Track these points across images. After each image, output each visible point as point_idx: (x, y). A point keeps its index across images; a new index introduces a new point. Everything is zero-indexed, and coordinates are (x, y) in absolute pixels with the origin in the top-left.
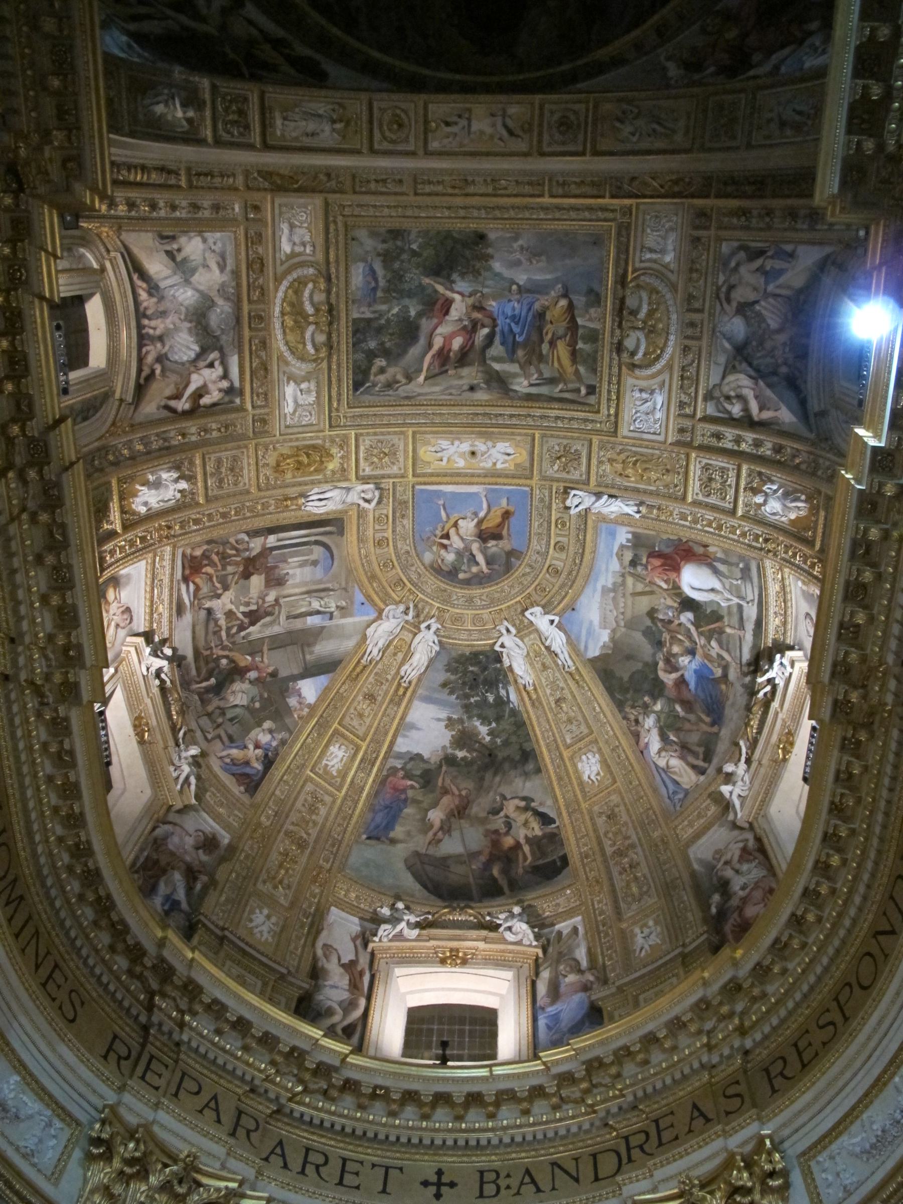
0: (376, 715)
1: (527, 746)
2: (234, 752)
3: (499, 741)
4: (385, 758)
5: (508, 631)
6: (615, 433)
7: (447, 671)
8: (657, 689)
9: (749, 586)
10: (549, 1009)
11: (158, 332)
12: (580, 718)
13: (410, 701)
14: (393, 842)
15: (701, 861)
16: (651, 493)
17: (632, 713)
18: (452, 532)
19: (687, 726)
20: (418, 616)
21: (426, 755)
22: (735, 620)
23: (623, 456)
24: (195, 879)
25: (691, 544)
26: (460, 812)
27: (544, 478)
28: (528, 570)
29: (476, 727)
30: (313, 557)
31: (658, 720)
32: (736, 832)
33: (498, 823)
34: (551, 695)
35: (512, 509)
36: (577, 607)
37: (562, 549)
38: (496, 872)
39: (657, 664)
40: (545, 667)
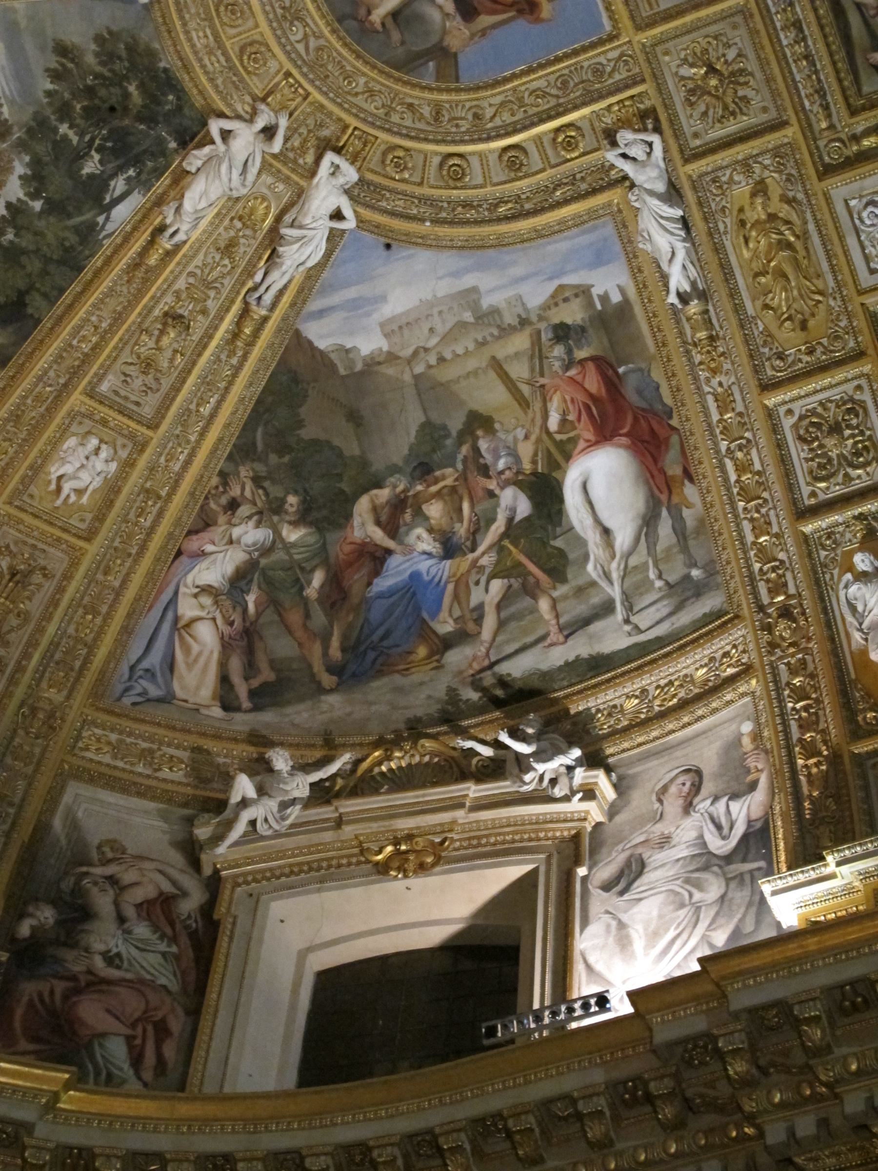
1: (35, 302)
3: (10, 236)
5: (269, 132)
6: (827, 171)
7: (99, 39)
9: (663, 608)
12: (166, 383)
15: (73, 825)
16: (739, 309)
19: (295, 617)
22: (574, 610)
23: (785, 211)
25: (675, 439)
27: (650, 53)
28: (426, 111)
29: (9, 170)
31: (267, 550)
32: (177, 858)
34: (177, 294)
36: (400, 252)
39: (379, 485)
40: (229, 249)
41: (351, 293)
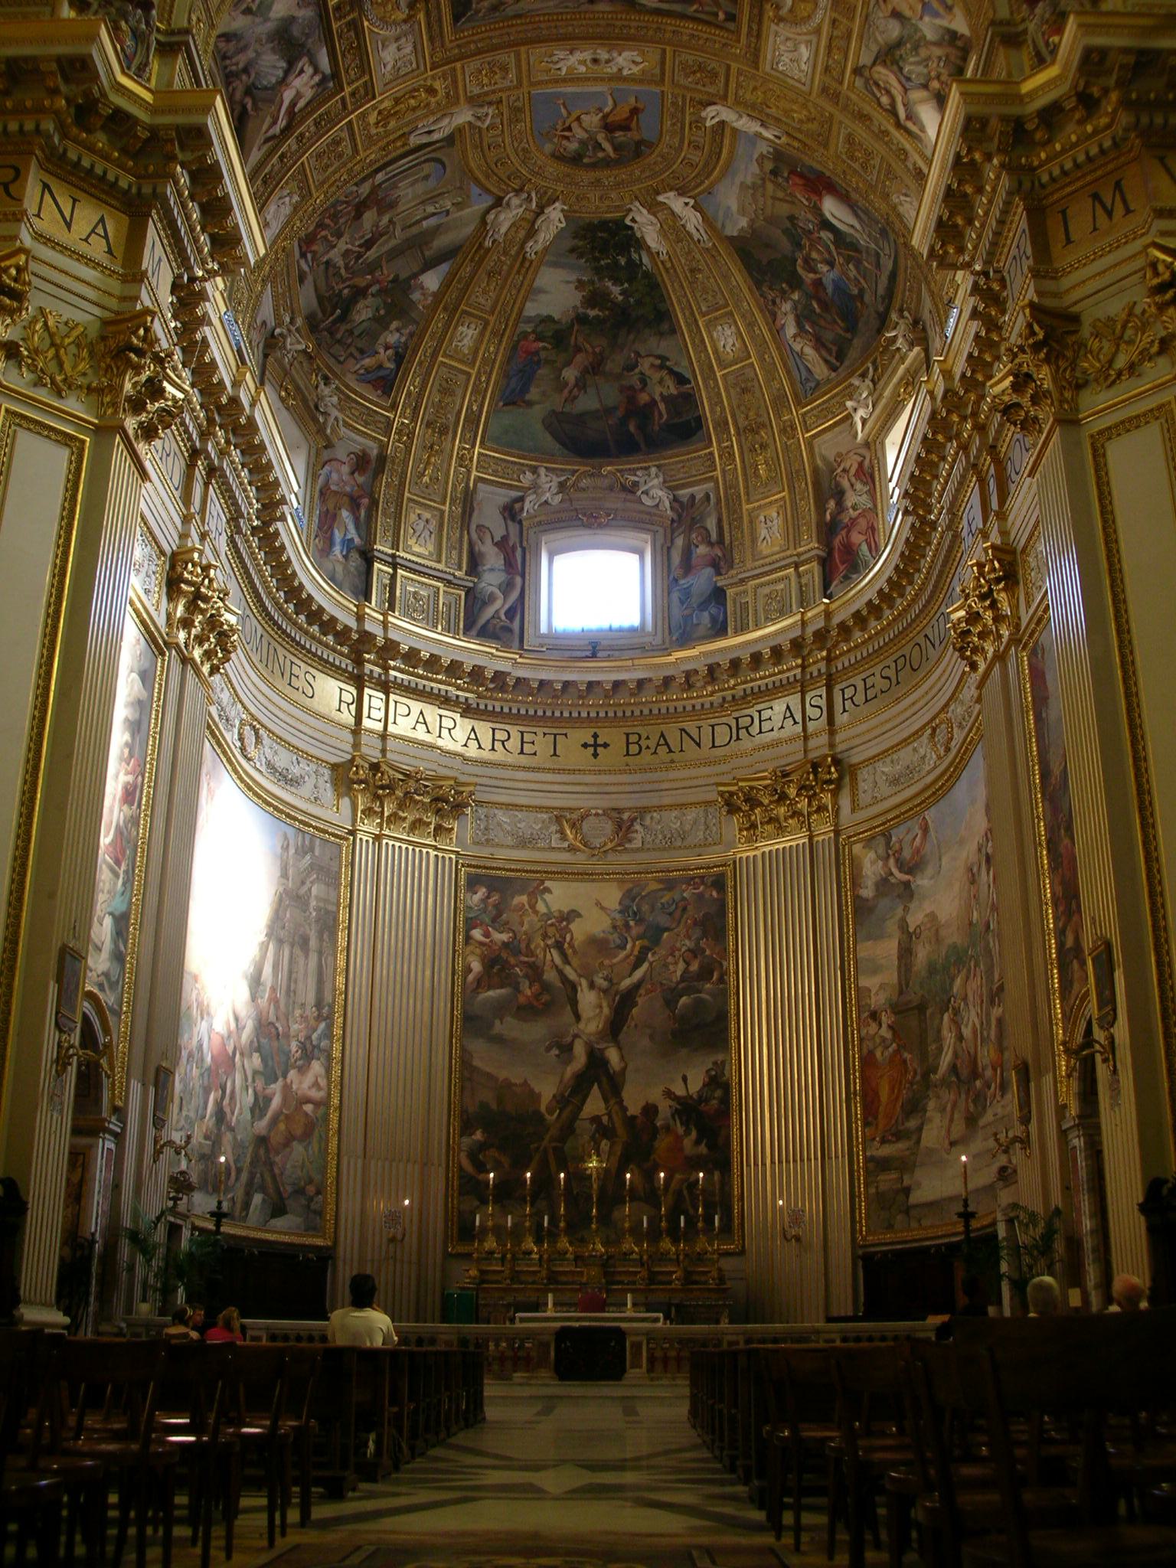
0: (502, 288)
2: (367, 362)
4: (516, 325)
6: (755, 63)
8: (795, 282)
10: (682, 582)
11: (241, 66)
13: (536, 272)
14: (530, 404)
15: (824, 459)
17: (771, 295)
18: (575, 125)
19: (822, 323)
20: (540, 199)
21: (556, 317)
22: (873, 259)
24: (358, 506)
26: (595, 368)
30: (422, 174)
31: (795, 308)
33: (634, 380)
35: (639, 105)
37: (697, 148)
38: (632, 428)
41: (721, 214)
